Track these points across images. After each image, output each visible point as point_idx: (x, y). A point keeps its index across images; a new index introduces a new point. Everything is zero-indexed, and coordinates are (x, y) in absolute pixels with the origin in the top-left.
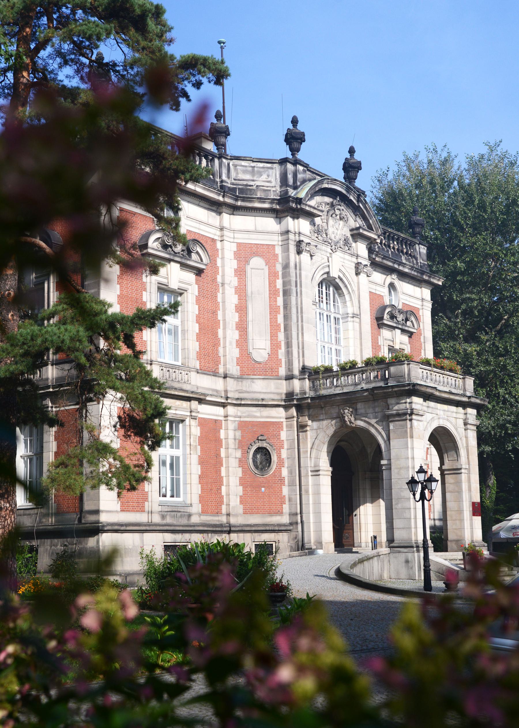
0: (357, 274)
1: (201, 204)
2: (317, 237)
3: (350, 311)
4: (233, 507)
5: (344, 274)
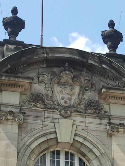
0: (110, 136)
2: (36, 106)
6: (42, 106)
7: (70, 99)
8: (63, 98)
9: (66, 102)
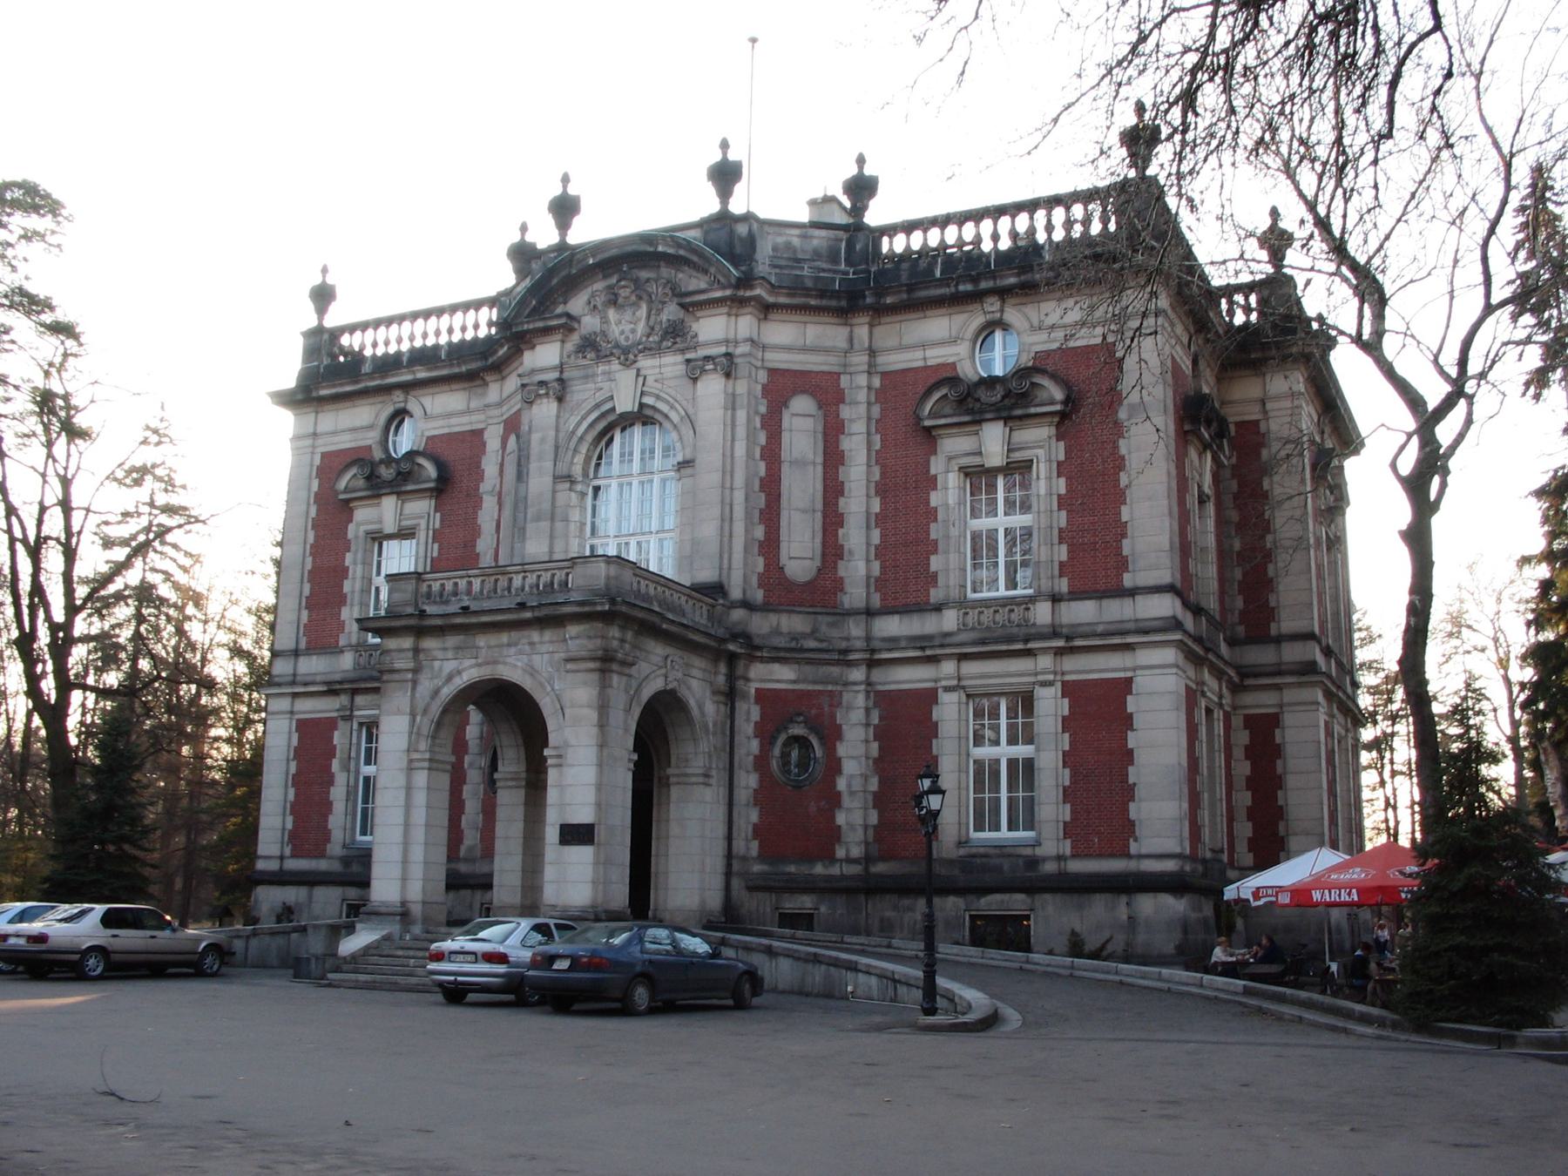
0: (695, 380)
1: (454, 386)
3: (680, 458)
4: (471, 849)
5: (658, 397)
7: (633, 331)
8: (622, 332)
9: (627, 339)
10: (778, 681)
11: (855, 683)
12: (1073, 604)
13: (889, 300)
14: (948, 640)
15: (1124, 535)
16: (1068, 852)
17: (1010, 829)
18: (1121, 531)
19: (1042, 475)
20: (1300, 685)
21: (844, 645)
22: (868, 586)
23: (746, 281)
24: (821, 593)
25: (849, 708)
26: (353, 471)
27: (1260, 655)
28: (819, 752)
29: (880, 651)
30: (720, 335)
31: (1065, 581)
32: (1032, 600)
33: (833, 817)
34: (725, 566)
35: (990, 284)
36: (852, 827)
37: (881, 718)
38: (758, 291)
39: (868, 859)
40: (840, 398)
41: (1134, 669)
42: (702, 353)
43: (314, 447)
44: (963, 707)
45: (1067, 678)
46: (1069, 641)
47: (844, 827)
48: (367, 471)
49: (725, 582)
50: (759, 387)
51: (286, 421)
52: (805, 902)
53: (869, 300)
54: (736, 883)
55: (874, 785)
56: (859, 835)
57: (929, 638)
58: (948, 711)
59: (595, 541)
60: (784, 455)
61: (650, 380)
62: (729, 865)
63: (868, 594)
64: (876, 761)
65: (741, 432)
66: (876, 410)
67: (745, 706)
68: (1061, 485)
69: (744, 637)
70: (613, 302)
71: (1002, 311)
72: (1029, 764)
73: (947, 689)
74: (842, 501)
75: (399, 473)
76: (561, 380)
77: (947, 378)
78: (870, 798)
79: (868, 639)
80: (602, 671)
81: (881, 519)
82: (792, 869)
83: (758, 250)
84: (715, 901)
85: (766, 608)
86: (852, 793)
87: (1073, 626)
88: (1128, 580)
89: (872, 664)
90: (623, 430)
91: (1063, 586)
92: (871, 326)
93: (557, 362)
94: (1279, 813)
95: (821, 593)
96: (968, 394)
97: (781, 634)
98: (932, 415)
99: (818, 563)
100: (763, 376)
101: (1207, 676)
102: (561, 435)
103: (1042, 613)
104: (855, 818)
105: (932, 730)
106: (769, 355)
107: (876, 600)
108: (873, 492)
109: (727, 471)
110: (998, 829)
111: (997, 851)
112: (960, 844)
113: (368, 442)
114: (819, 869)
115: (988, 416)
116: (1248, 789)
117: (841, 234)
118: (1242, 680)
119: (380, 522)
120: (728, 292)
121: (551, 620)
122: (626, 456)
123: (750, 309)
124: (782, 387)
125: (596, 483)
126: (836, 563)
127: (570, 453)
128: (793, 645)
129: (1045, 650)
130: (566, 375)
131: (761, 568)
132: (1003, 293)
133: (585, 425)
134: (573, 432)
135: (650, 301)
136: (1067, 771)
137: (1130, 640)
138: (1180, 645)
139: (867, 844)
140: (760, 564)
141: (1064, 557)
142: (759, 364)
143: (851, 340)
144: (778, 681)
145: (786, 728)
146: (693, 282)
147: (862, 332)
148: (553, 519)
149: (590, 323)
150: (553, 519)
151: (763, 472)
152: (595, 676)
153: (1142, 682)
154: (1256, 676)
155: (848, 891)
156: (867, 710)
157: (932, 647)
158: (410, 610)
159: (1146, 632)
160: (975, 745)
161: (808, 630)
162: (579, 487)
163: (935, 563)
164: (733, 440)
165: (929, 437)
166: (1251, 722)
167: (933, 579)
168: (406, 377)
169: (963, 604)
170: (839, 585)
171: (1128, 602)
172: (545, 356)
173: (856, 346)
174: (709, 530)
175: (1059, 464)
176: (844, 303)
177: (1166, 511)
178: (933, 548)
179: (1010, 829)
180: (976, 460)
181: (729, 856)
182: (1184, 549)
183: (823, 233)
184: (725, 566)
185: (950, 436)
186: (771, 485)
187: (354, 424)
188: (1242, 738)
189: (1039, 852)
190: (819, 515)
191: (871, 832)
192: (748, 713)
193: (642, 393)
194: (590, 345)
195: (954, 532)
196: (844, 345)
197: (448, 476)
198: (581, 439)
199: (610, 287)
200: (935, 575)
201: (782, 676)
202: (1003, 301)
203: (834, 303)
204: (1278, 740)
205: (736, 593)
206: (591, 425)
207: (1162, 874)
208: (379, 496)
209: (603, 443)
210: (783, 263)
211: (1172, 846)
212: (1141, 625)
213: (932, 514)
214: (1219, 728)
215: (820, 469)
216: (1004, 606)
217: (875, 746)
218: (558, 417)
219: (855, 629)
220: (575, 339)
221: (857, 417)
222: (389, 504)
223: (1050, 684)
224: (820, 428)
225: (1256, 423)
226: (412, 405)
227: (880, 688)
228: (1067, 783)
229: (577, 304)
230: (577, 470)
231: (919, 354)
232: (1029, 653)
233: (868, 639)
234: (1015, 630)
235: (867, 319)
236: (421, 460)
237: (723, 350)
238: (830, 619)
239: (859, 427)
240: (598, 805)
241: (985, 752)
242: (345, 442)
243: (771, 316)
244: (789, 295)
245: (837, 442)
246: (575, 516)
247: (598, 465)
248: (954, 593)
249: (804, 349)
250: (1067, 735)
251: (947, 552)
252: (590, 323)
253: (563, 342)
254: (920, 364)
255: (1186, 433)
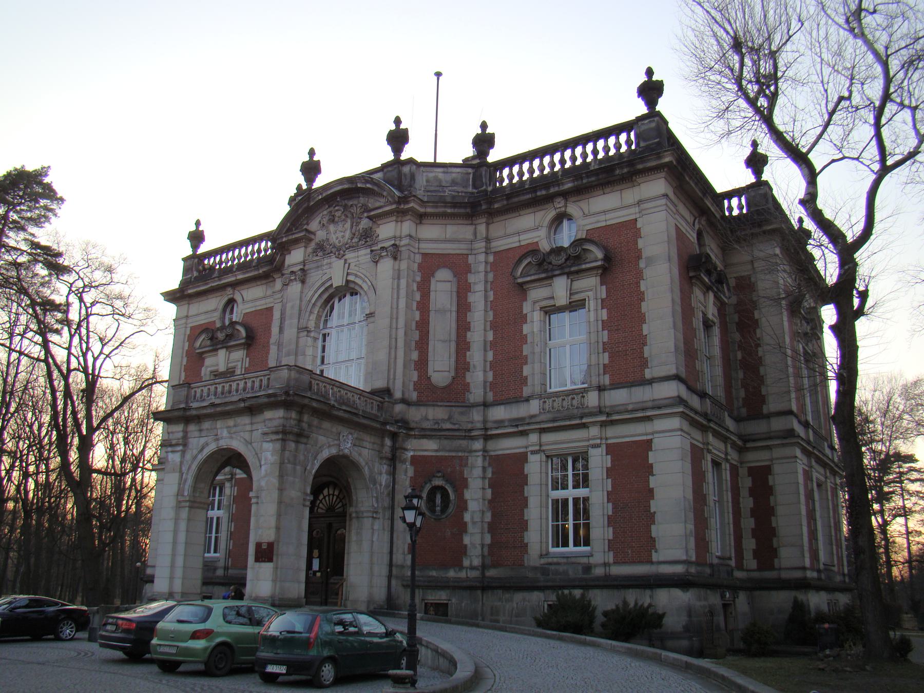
0: (376, 262)
5: (356, 276)
6: (320, 254)
7: (343, 237)
9: (340, 242)
10: (426, 450)
11: (475, 451)
12: (612, 391)
13: (496, 206)
14: (533, 420)
15: (645, 344)
16: (611, 560)
17: (575, 545)
18: (642, 341)
19: (592, 308)
20: (783, 445)
21: (469, 426)
22: (485, 388)
23: (403, 200)
24: (454, 393)
25: (473, 467)
26: (203, 337)
27: (756, 427)
28: (452, 496)
29: (491, 429)
30: (391, 234)
31: (607, 377)
32: (585, 390)
33: (462, 540)
34: (392, 377)
35: (556, 189)
36: (473, 545)
37: (493, 473)
38: (411, 205)
39: (484, 567)
40: (468, 269)
41: (652, 434)
42: (380, 246)
43: (186, 324)
44: (544, 464)
45: (609, 441)
46: (610, 418)
47: (469, 546)
48: (210, 335)
49: (391, 386)
50: (416, 265)
51: (171, 310)
52: (441, 596)
53: (484, 207)
54: (394, 582)
55: (488, 517)
56: (478, 551)
57: (522, 419)
58: (534, 467)
59: (323, 367)
60: (432, 307)
61: (352, 266)
62: (390, 571)
63: (485, 393)
64: (490, 502)
65: (403, 292)
66: (491, 276)
67: (404, 466)
68: (604, 314)
69: (404, 423)
70: (332, 220)
71: (566, 206)
72: (586, 500)
73: (533, 452)
74: (469, 334)
75: (227, 336)
76: (302, 270)
77: (532, 251)
78: (486, 526)
79: (485, 421)
80: (283, 440)
81: (493, 345)
82: (434, 573)
83: (417, 181)
84: (380, 594)
85: (418, 404)
86: (474, 523)
87: (611, 406)
88: (648, 374)
89: (487, 438)
90: (340, 300)
91: (607, 380)
92: (488, 224)
93: (302, 259)
94: (773, 532)
95: (454, 393)
96: (544, 260)
97: (428, 420)
98: (522, 276)
99: (453, 374)
100: (418, 259)
101: (711, 438)
102: (304, 303)
103: (592, 399)
104: (475, 539)
105: (524, 480)
106: (422, 245)
107: (490, 397)
108: (488, 328)
109: (394, 318)
110: (565, 544)
111: (565, 560)
112: (541, 556)
113: (214, 319)
114: (452, 574)
115: (557, 272)
116: (752, 517)
117: (470, 170)
118: (745, 444)
119: (217, 365)
120: (394, 206)
121: (252, 409)
122: (341, 316)
123: (408, 217)
124: (430, 264)
125: (326, 331)
126: (464, 374)
127: (308, 314)
128: (436, 427)
129: (594, 423)
130: (307, 267)
131: (415, 378)
132: (565, 195)
133: (316, 296)
134: (310, 301)
135: (353, 217)
136: (610, 505)
137: (649, 413)
138: (683, 415)
139: (483, 556)
140: (415, 376)
141: (606, 361)
142: (416, 251)
143: (475, 234)
144: (426, 450)
145: (430, 481)
146: (372, 203)
147: (482, 228)
148: (296, 355)
149: (321, 235)
150: (296, 355)
151: (418, 318)
152: (278, 445)
153: (657, 443)
154: (754, 441)
155: (471, 588)
156: (484, 469)
157: (522, 425)
158: (183, 406)
159: (659, 408)
160: (553, 489)
161: (446, 417)
162: (312, 334)
163: (526, 370)
164: (398, 298)
165: (522, 289)
166: (752, 471)
167: (524, 381)
168: (230, 279)
169: (544, 396)
170: (466, 387)
171: (647, 388)
172: (296, 257)
173: (479, 237)
174: (382, 355)
175: (603, 300)
176: (468, 210)
177: (672, 326)
178: (525, 360)
179: (575, 545)
180: (551, 302)
181: (391, 565)
182: (689, 353)
183: (458, 170)
184: (392, 377)
185: (534, 288)
186: (423, 326)
187: (208, 310)
188: (746, 483)
189: (592, 560)
190: (453, 345)
191: (486, 550)
192: (406, 471)
193: (348, 274)
194: (320, 247)
195: (537, 350)
196: (471, 237)
197: (252, 337)
198: (314, 304)
199: (331, 212)
200: (526, 378)
201: (429, 447)
202: (566, 200)
203: (462, 211)
204: (771, 483)
205: (398, 395)
206: (320, 296)
207: (674, 575)
208: (216, 350)
209: (328, 307)
210: (432, 188)
211: (680, 555)
212: (656, 403)
213: (524, 339)
214: (726, 475)
215: (454, 314)
216: (567, 395)
217: (489, 491)
218: (302, 292)
219: (477, 416)
220: (313, 245)
221: (478, 280)
222: (222, 353)
223: (598, 446)
224: (455, 289)
225: (749, 277)
226: (238, 297)
227: (492, 453)
228: (610, 513)
229: (314, 225)
230: (312, 325)
231: (516, 239)
232: (584, 426)
233: (485, 421)
234: (575, 411)
235: (484, 220)
236: (239, 327)
237: (393, 242)
238: (460, 410)
239: (480, 287)
240: (278, 528)
241: (560, 494)
242: (202, 320)
243: (424, 222)
244: (432, 207)
245: (466, 298)
246: (309, 352)
247: (326, 321)
248: (538, 389)
249: (446, 241)
250: (610, 481)
251: (533, 363)
252: (321, 235)
253: (306, 247)
254: (517, 244)
255: (691, 278)
